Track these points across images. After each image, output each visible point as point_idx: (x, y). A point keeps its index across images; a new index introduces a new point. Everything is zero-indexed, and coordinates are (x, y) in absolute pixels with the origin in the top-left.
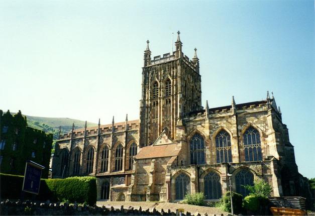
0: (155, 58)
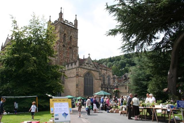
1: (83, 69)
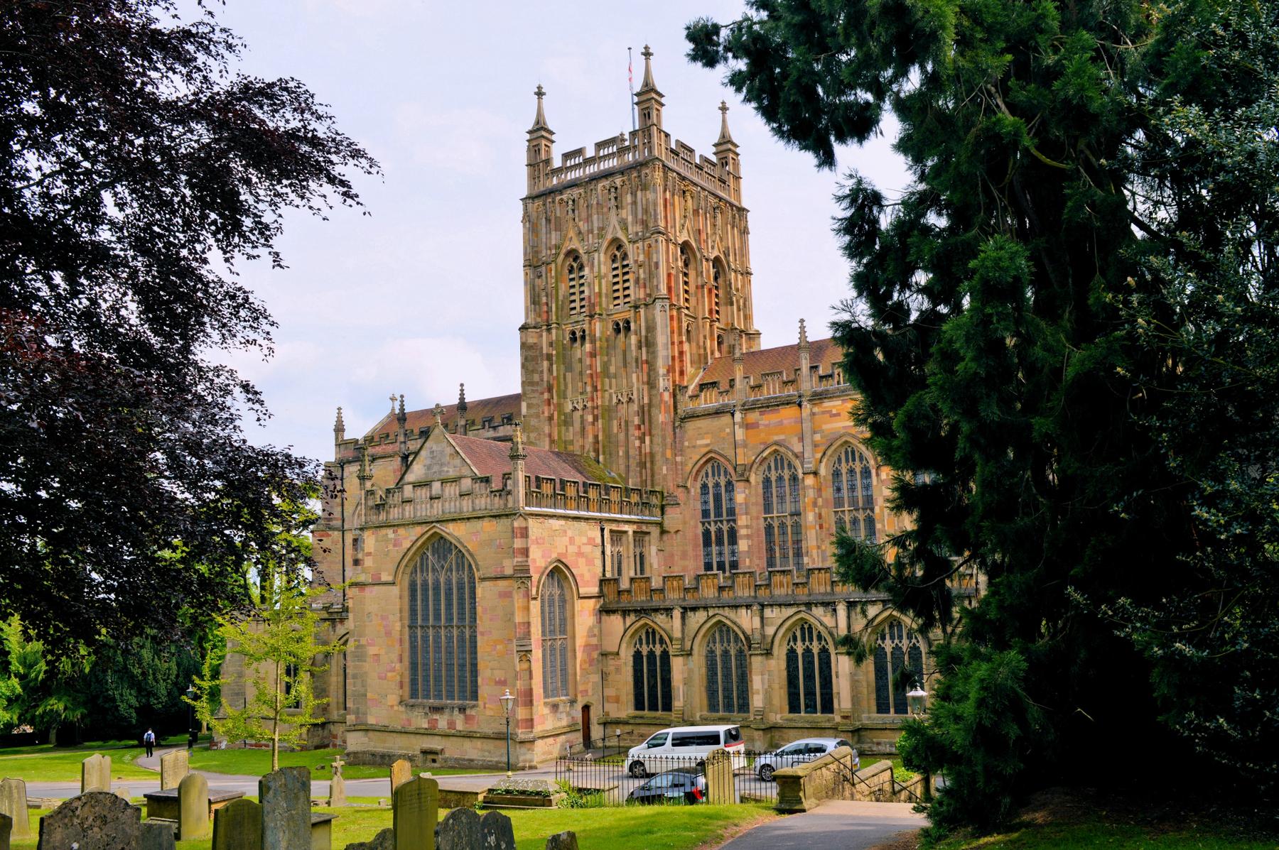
0: (567, 156)
1: (390, 533)
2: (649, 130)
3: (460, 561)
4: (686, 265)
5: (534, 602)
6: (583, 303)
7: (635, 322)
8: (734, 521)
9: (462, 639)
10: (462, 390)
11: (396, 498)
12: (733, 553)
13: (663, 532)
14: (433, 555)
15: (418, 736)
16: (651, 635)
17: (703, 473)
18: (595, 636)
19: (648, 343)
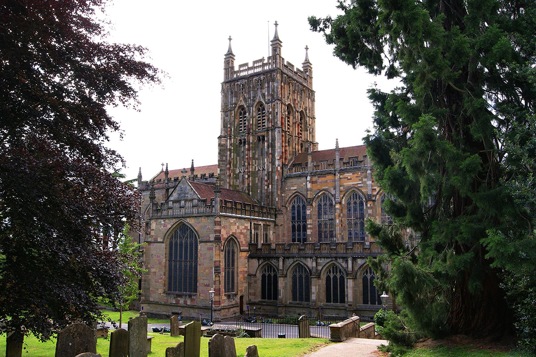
0: (240, 66)
2: (276, 57)
3: (191, 234)
4: (289, 113)
5: (222, 252)
6: (245, 128)
7: (267, 137)
8: (306, 222)
9: (191, 267)
10: (193, 162)
11: (165, 207)
12: (304, 235)
13: (276, 225)
14: (180, 231)
15: (171, 307)
16: (270, 267)
17: (293, 201)
18: (246, 267)
19: (272, 146)
